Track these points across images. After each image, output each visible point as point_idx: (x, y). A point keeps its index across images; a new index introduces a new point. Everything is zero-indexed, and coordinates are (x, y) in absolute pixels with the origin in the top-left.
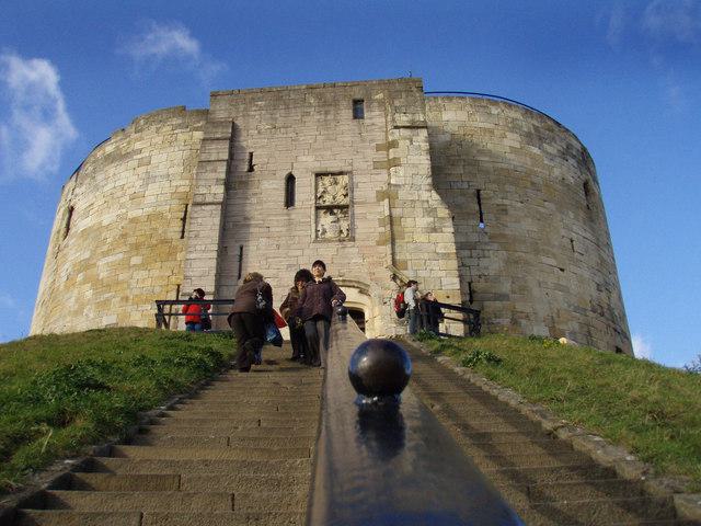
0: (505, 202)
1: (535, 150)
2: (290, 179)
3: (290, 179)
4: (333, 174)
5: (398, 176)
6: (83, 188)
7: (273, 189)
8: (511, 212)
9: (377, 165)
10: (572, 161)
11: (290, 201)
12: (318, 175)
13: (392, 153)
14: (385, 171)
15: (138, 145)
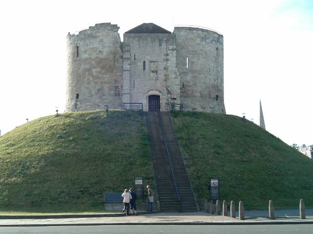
0: (194, 60)
1: (204, 43)
2: (144, 62)
3: (144, 62)
4: (154, 62)
5: (169, 63)
6: (81, 43)
7: (141, 64)
8: (195, 63)
9: (164, 60)
10: (214, 43)
11: (144, 69)
12: (151, 62)
13: (168, 57)
14: (166, 62)
15: (98, 34)
